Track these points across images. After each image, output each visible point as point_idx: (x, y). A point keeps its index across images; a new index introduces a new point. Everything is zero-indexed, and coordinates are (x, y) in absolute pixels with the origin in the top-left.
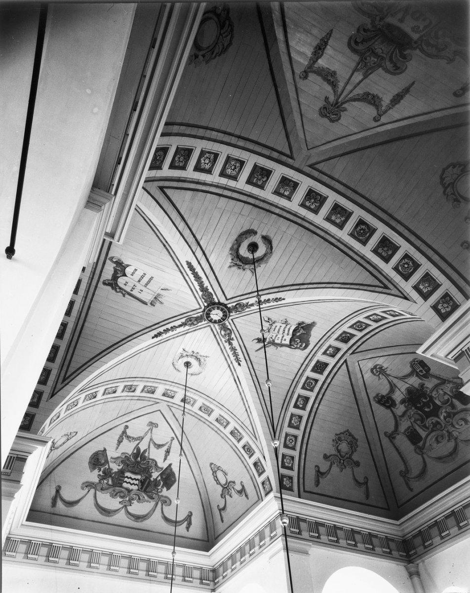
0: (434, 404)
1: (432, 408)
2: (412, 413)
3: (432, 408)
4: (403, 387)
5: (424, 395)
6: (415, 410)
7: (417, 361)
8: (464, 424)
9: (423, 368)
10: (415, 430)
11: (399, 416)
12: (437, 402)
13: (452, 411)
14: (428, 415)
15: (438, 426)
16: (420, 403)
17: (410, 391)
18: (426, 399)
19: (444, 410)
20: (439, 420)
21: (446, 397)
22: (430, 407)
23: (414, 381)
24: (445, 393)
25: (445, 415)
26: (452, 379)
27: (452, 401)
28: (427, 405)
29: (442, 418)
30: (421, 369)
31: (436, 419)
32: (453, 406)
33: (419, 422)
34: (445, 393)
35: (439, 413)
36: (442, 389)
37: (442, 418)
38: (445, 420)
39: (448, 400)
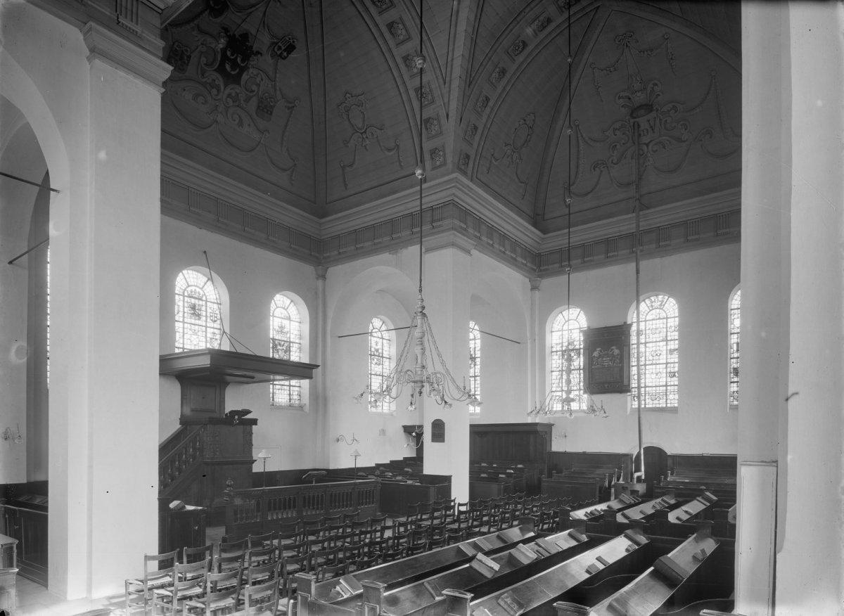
0: (239, 75)
1: (233, 73)
2: (213, 46)
3: (233, 73)
4: (250, 26)
5: (246, 58)
6: (219, 50)
7: (294, 42)
8: (236, 122)
9: (285, 50)
10: (189, 57)
11: (198, 26)
12: (245, 77)
13: (242, 102)
14: (221, 70)
15: (214, 91)
16: (232, 55)
17: (245, 36)
18: (243, 61)
19: (237, 90)
20: (222, 87)
21: (254, 88)
22: (234, 71)
23: (262, 41)
24: (258, 85)
25: (233, 95)
26: (278, 88)
27: (253, 96)
28: (234, 65)
29: (227, 91)
30: (283, 48)
31: (220, 81)
32: (247, 100)
33: (204, 60)
34: (260, 85)
35: (231, 86)
36: (262, 80)
37: (227, 91)
38: (228, 97)
39: (254, 91)
